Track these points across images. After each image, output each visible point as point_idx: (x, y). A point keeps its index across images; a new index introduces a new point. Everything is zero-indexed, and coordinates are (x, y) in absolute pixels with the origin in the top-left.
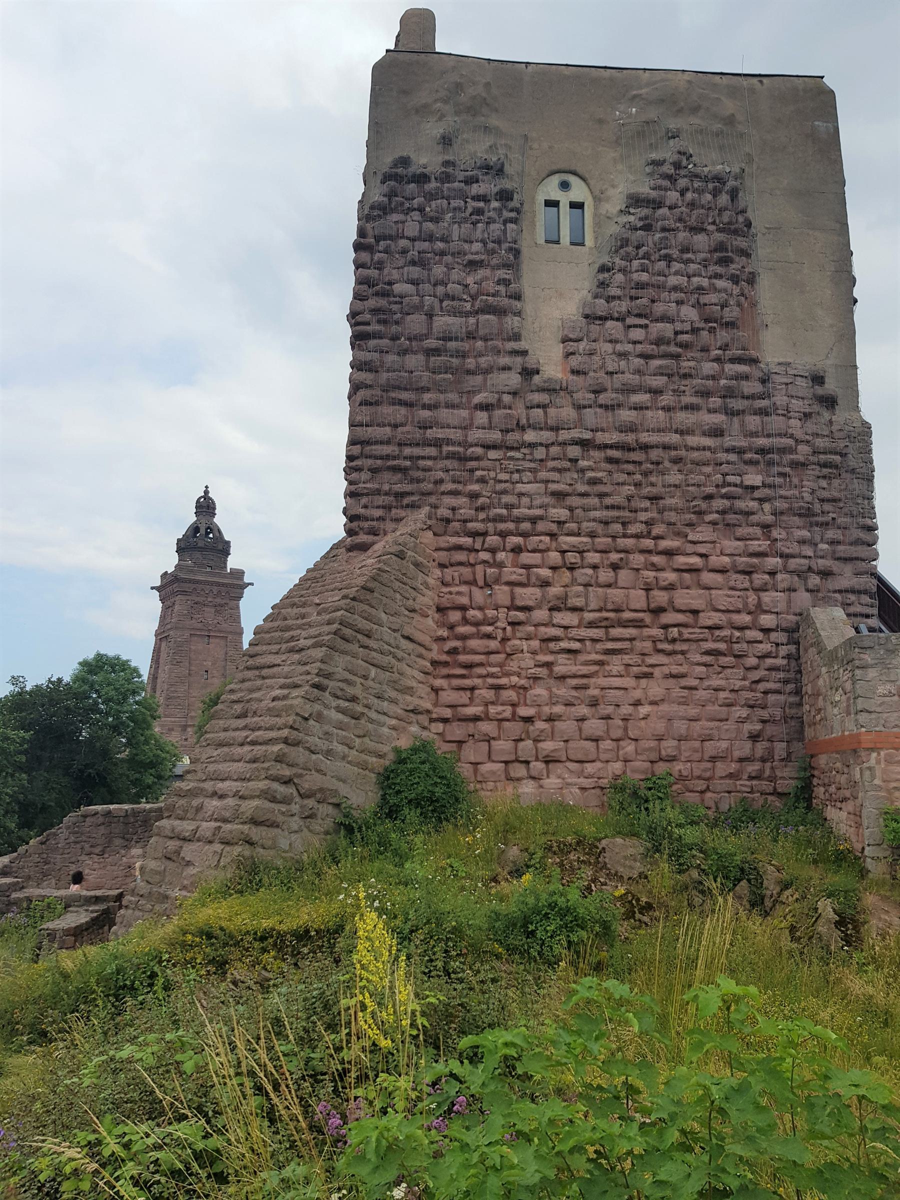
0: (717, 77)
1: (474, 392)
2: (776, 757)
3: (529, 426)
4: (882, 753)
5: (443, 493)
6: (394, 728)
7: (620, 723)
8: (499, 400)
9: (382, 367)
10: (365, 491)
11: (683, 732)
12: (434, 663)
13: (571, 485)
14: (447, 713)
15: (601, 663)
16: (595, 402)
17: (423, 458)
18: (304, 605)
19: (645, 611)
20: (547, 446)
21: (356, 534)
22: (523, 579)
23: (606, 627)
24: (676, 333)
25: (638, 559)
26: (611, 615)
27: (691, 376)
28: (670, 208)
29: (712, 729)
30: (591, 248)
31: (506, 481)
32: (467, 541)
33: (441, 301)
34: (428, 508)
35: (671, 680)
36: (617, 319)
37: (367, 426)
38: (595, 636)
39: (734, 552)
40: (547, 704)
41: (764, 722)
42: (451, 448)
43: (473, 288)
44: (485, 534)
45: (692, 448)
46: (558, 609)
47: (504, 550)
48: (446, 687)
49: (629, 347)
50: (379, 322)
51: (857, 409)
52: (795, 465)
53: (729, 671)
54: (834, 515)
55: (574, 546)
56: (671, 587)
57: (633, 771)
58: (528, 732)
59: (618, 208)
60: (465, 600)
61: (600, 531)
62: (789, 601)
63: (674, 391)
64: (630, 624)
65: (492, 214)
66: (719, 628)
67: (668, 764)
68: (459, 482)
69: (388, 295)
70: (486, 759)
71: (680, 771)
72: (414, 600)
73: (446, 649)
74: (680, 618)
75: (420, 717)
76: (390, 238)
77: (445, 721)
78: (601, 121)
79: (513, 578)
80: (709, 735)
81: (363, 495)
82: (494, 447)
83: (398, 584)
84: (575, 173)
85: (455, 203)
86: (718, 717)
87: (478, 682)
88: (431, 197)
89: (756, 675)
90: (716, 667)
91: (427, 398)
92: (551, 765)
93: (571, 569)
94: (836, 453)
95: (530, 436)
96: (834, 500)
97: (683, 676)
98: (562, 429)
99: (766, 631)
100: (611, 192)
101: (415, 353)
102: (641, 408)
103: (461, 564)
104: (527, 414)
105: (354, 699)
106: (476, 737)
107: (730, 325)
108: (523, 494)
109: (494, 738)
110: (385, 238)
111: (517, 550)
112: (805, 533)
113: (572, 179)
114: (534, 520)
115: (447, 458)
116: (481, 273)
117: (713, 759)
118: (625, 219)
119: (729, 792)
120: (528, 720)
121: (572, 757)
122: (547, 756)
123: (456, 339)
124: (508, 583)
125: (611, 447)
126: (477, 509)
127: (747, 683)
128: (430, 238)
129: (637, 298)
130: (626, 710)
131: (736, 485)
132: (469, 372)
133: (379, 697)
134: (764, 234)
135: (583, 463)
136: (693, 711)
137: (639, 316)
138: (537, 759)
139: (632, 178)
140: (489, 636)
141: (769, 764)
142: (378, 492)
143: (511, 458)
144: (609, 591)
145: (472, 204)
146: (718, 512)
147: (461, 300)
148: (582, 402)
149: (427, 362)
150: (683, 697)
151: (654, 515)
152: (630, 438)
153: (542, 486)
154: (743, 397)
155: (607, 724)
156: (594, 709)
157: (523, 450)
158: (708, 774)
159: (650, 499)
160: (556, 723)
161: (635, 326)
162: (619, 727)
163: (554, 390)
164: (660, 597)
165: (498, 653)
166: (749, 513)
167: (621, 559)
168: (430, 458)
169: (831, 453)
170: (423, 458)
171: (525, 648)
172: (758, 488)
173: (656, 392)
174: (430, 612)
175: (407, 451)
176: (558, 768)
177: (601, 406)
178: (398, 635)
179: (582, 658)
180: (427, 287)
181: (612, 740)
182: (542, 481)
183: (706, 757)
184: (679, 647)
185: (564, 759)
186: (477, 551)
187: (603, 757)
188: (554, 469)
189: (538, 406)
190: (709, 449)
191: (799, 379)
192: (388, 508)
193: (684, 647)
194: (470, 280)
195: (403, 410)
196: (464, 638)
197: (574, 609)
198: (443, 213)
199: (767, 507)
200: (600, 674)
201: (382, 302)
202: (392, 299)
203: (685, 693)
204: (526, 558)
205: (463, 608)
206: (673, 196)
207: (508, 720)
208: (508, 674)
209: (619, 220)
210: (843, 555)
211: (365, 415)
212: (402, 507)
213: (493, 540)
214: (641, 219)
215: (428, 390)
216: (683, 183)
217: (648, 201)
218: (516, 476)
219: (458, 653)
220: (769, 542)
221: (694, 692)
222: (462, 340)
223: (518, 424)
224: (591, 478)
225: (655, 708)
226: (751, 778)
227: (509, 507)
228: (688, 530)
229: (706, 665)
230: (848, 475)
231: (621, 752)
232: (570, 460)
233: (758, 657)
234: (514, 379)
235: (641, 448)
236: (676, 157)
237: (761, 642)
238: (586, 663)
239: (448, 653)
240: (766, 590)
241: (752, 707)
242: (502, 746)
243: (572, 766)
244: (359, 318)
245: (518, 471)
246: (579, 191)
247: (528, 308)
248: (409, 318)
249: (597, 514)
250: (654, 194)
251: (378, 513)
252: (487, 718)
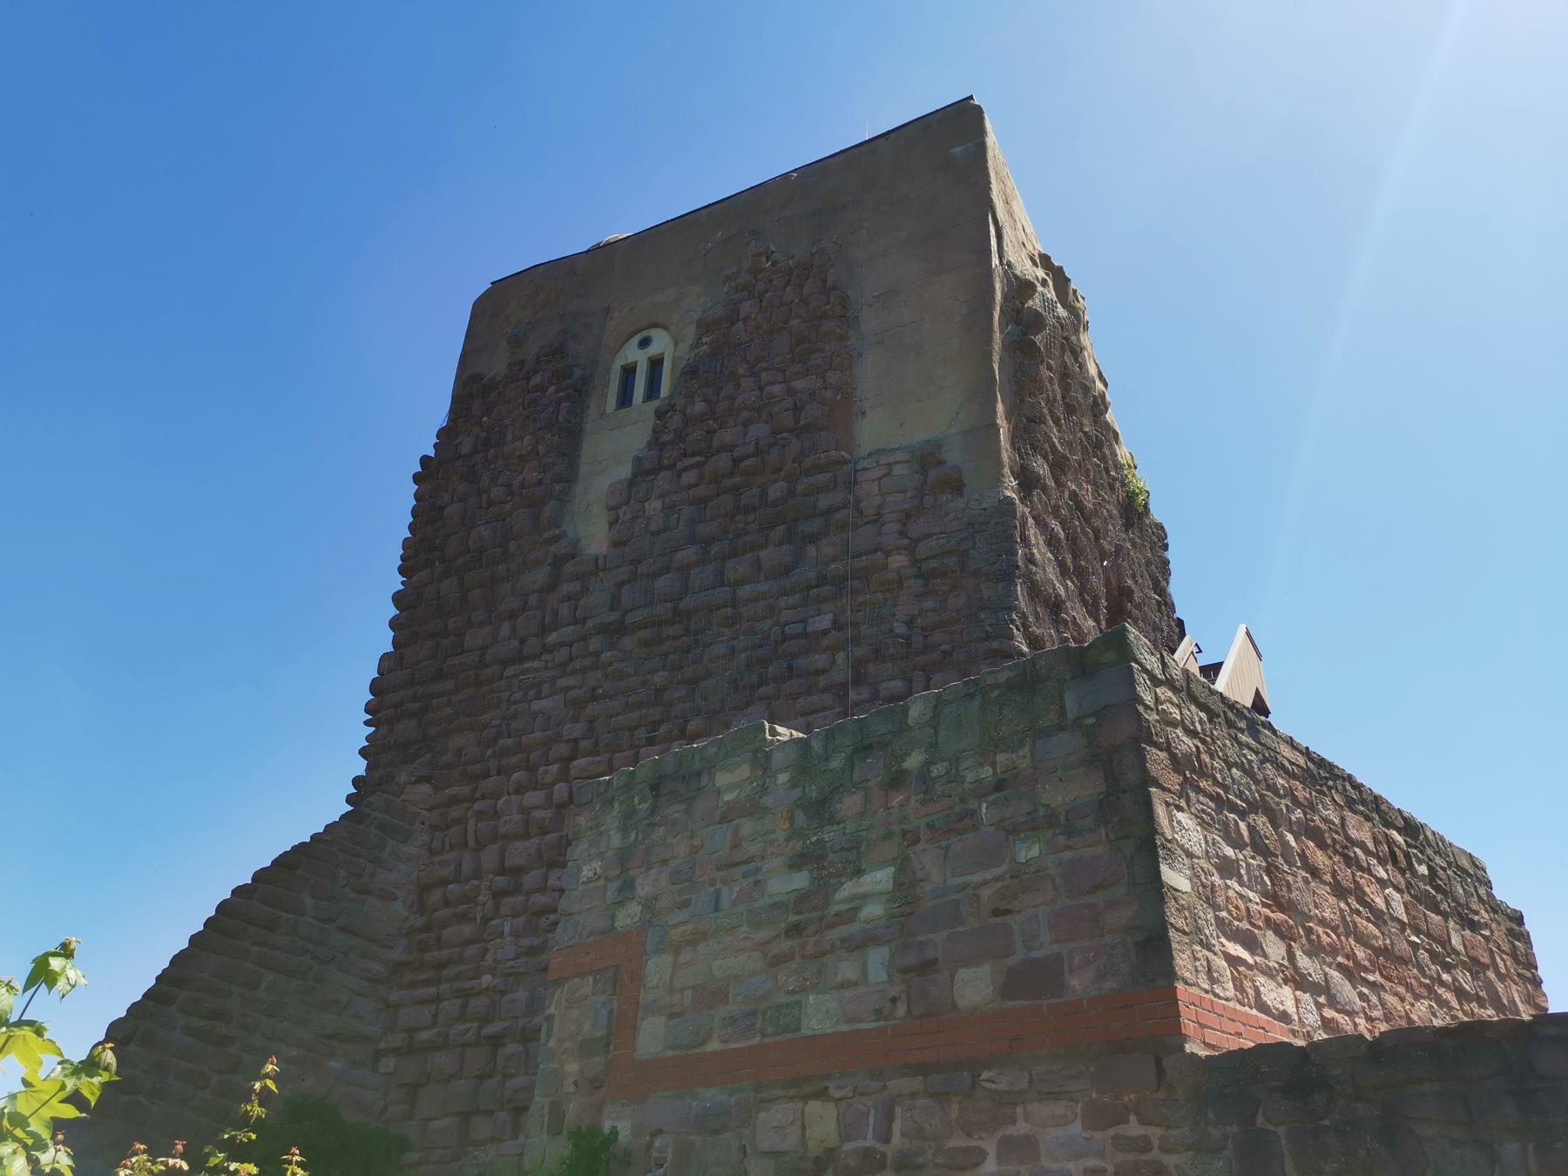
24: (734, 460)
32: (465, 790)
77: (397, 1051)
84: (655, 325)
120: (497, 1041)
161: (686, 469)
199: (840, 657)
246: (661, 343)
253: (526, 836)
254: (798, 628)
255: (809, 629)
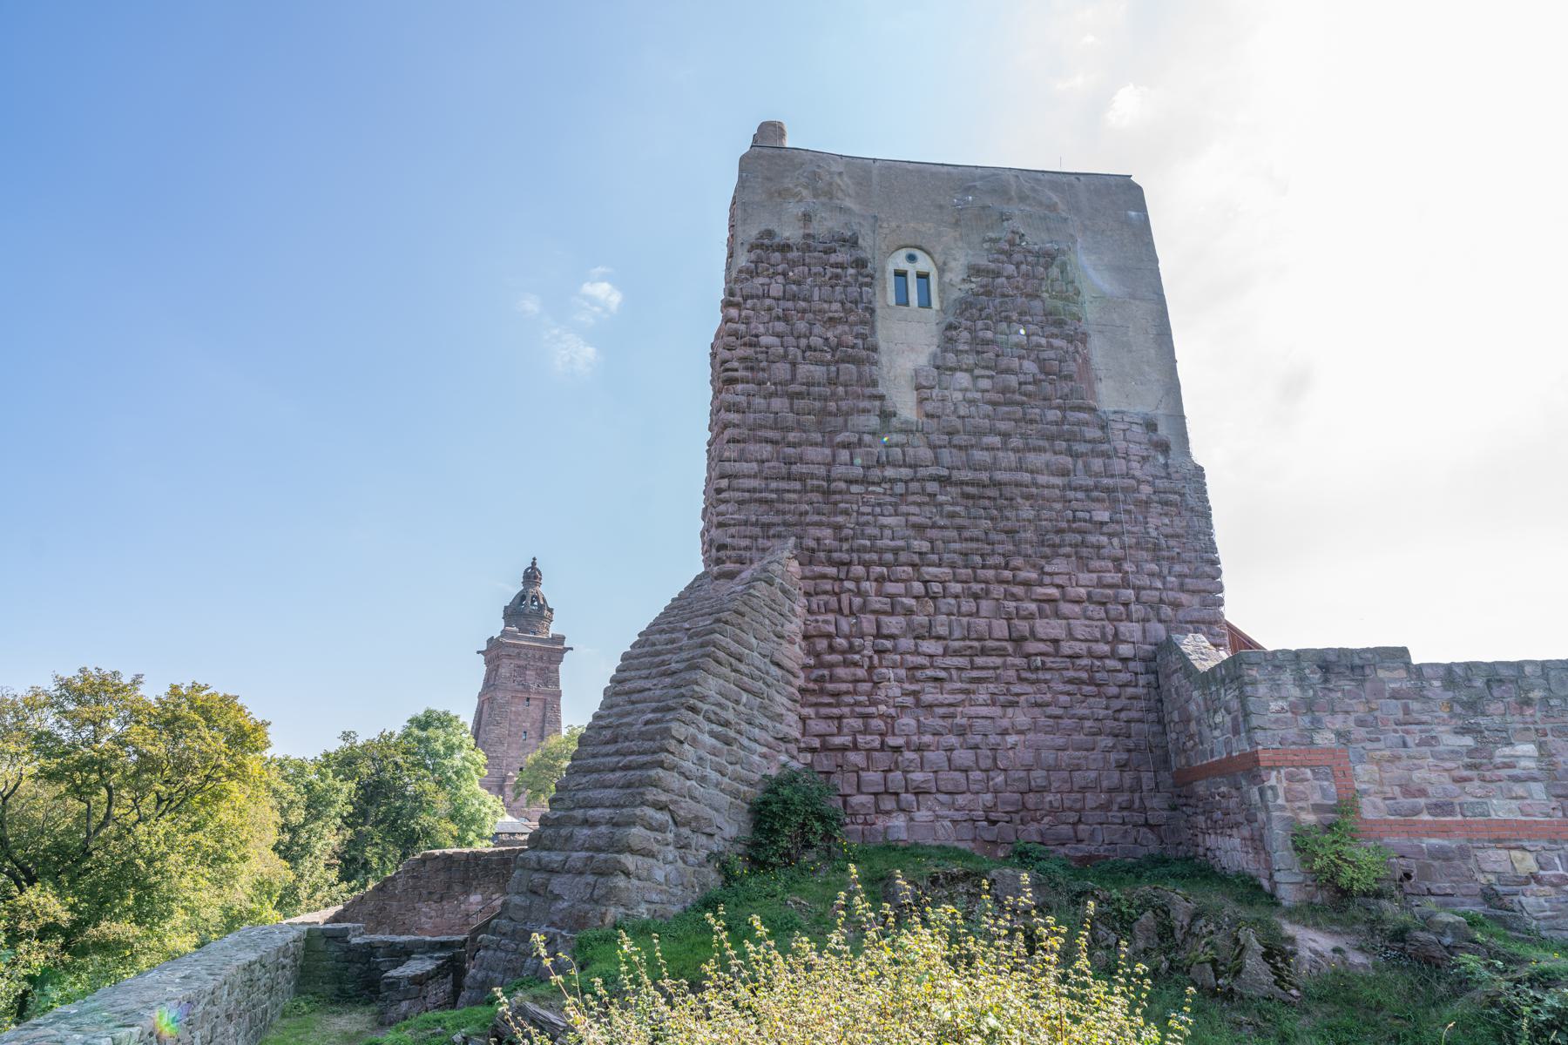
0: (1040, 174)
1: (835, 432)
2: (1144, 788)
3: (889, 463)
4: (1282, 771)
5: (808, 524)
6: (764, 756)
7: (989, 753)
8: (860, 440)
9: (749, 408)
10: (733, 522)
11: (1052, 762)
12: (802, 691)
13: (930, 518)
14: (816, 743)
15: (966, 692)
16: (950, 442)
17: (789, 491)
18: (673, 631)
19: (1006, 640)
20: (906, 482)
21: (723, 562)
22: (888, 608)
23: (971, 656)
24: (1020, 384)
25: (998, 590)
26: (976, 644)
27: (1036, 422)
28: (1008, 278)
29: (1079, 759)
30: (937, 311)
31: (868, 514)
32: (832, 571)
33: (804, 352)
34: (793, 539)
35: (1036, 709)
36: (966, 371)
37: (735, 461)
38: (960, 665)
39: (1088, 583)
40: (915, 734)
41: (1129, 751)
42: (815, 482)
43: (833, 341)
44: (850, 564)
45: (1043, 486)
46: (923, 638)
47: (868, 579)
48: (813, 716)
49: (978, 395)
50: (746, 369)
51: (1187, 454)
52: (1138, 503)
53: (1092, 699)
54: (1178, 550)
55: (936, 576)
56: (1031, 616)
57: (1004, 803)
58: (896, 763)
59: (960, 277)
60: (832, 629)
61: (960, 563)
62: (1144, 631)
63: (1021, 434)
64: (993, 653)
65: (849, 278)
66: (1079, 657)
67: (1038, 795)
68: (824, 514)
69: (755, 346)
70: (855, 792)
71: (1051, 802)
72: (782, 626)
73: (813, 676)
74: (1042, 647)
75: (789, 746)
76: (758, 297)
77: (813, 750)
78: (941, 207)
79: (877, 606)
80: (1078, 765)
81: (730, 525)
82: (856, 482)
83: (767, 609)
85: (814, 270)
86: (1085, 747)
87: (846, 710)
88: (793, 264)
89: (1117, 704)
90: (1079, 696)
91: (792, 436)
92: (920, 797)
93: (934, 598)
94: (1175, 493)
95: (890, 472)
96: (1178, 536)
97: (1048, 705)
98: (921, 466)
99: (1124, 660)
100: (953, 264)
101: (782, 396)
102: (993, 449)
103: (826, 593)
104: (887, 453)
105: (727, 724)
106: (845, 767)
107: (1069, 377)
108: (886, 526)
109: (862, 769)
110: (752, 297)
111: (881, 580)
112: (1154, 567)
113: (918, 253)
114: (896, 551)
115: (812, 491)
116: (840, 329)
117: (1083, 790)
118: (966, 286)
119: (1101, 824)
120: (897, 749)
121: (943, 789)
122: (918, 787)
123: (819, 385)
124: (874, 612)
125: (967, 484)
126: (841, 540)
127: (1110, 712)
128: (794, 298)
129: (984, 352)
130: (993, 739)
131: (1085, 521)
132: (830, 414)
133: (750, 724)
134: (1091, 302)
135: (941, 498)
136: (1060, 741)
137: (987, 368)
138: (907, 791)
139: (971, 252)
140: (855, 664)
141: (1137, 796)
142: (746, 523)
143: (873, 493)
144: (972, 620)
145: (830, 271)
146: (1070, 545)
147: (822, 351)
148: (937, 443)
149: (792, 405)
150: (1049, 726)
151: (1011, 547)
152: (984, 476)
153: (903, 519)
154: (1085, 441)
155: (976, 754)
156: (961, 739)
157: (883, 485)
158: (1078, 805)
159: (1006, 532)
160: (925, 753)
161: (983, 377)
162: (988, 757)
163: (912, 431)
164: (1023, 626)
165: (864, 681)
166: (1099, 547)
167: (982, 589)
168: (794, 491)
169: (1170, 492)
170: (789, 491)
171: (892, 676)
172: (1106, 523)
173: (1006, 435)
174: (797, 640)
175: (774, 485)
176: (929, 800)
177: (955, 446)
178: (767, 660)
179: (948, 686)
180: (790, 340)
181: (982, 770)
182: (903, 514)
183: (1076, 788)
184: (1041, 675)
185: (934, 790)
186: (842, 580)
187: (974, 787)
188: (914, 503)
189: (897, 446)
190: (1058, 487)
191: (1134, 426)
192: (754, 538)
193: (1048, 676)
194: (829, 334)
195: (769, 447)
196: (831, 666)
197: (939, 638)
198: (804, 278)
199: (1116, 541)
200: (967, 703)
201: (749, 351)
202: (758, 349)
203: (1051, 722)
204: (891, 588)
205: (829, 636)
206: (1011, 269)
207: (876, 750)
208: (874, 703)
209: (962, 287)
210: (1191, 588)
211: (731, 452)
212: (768, 537)
213: (859, 570)
214: (982, 286)
215: (793, 429)
216: (1017, 257)
217: (988, 272)
218: (878, 510)
219: (824, 681)
220: (1120, 575)
221: (1060, 721)
222: (824, 386)
223: (878, 461)
224: (949, 512)
225: (1022, 737)
226: (1121, 809)
227: (872, 538)
228: (1043, 562)
229: (1068, 694)
230: (1189, 514)
231: (991, 783)
232: (929, 495)
233: (1119, 686)
234: (874, 421)
235: (995, 485)
236: (1010, 236)
237: (1120, 671)
238: (952, 692)
239: (816, 681)
240: (1121, 621)
241: (1117, 736)
242: (873, 777)
243: (941, 797)
244: (728, 365)
245: (879, 505)
246: (924, 264)
247: (884, 359)
248: (774, 366)
249: (957, 546)
250: (992, 266)
251: (747, 542)
252: (856, 747)
253: (892, 613)
254: (1087, 516)
255: (1095, 519)
